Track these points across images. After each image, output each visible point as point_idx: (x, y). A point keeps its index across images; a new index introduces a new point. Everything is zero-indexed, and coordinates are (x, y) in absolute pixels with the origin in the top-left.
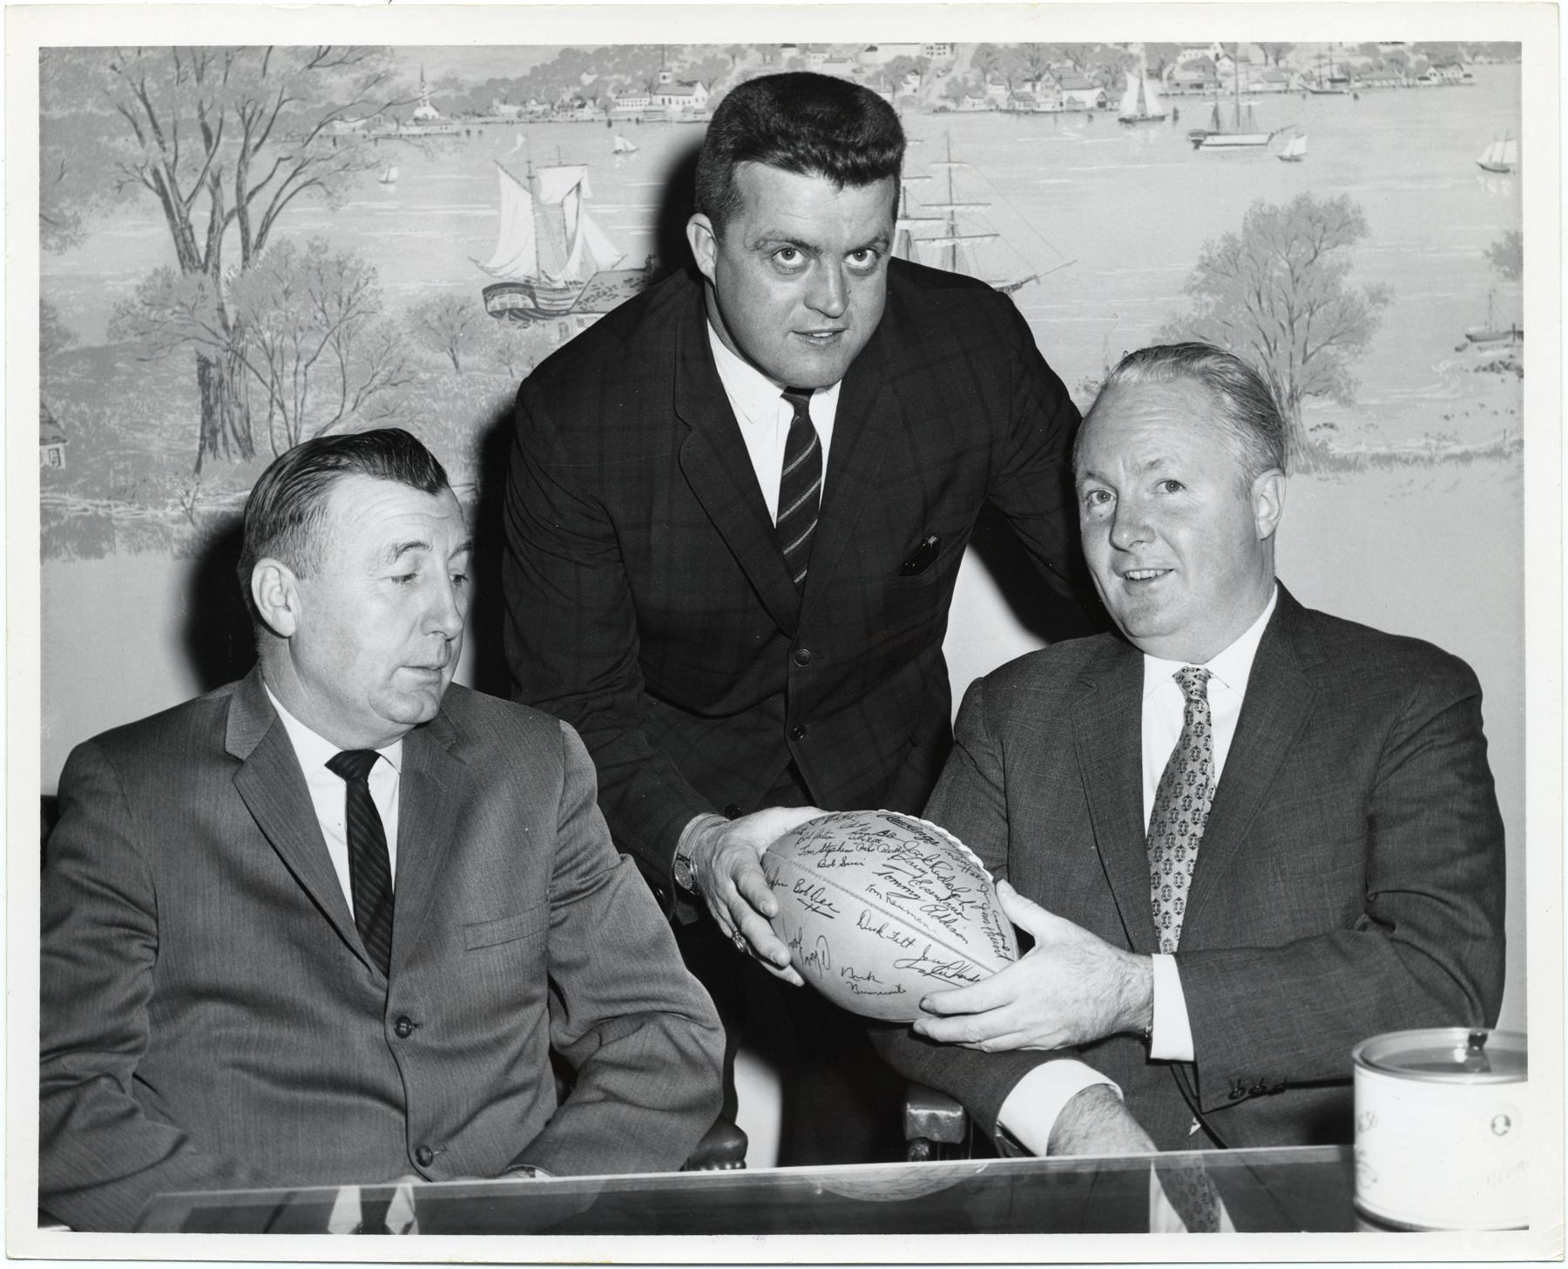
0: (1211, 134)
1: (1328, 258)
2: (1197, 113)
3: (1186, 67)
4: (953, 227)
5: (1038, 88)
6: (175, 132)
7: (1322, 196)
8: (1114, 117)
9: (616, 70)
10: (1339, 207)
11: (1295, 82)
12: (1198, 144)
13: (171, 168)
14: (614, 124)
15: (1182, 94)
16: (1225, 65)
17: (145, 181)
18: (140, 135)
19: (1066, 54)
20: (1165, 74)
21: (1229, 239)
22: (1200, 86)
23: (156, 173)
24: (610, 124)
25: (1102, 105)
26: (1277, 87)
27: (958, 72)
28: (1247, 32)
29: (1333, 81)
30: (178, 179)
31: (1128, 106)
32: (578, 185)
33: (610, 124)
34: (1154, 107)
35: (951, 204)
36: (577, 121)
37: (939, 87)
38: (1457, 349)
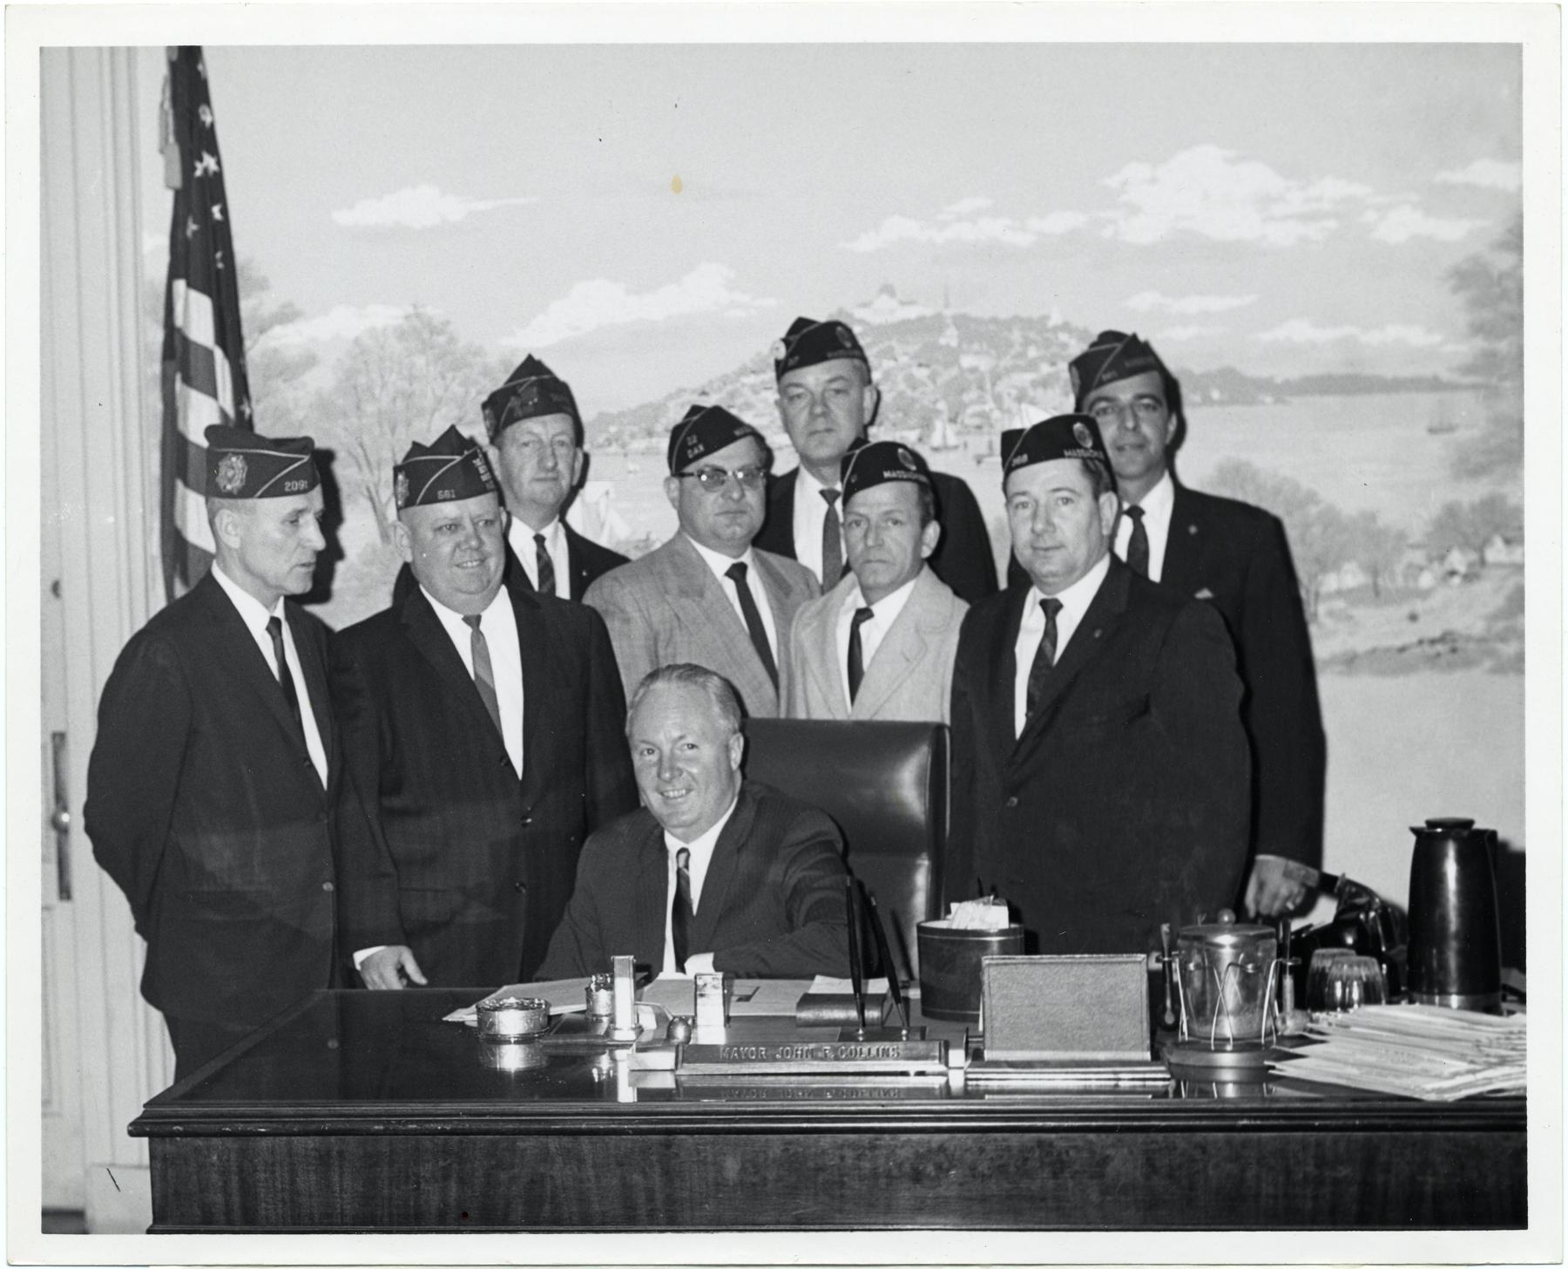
3: (975, 415)
6: (379, 465)
9: (629, 424)
12: (979, 462)
13: (376, 485)
14: (630, 456)
15: (969, 433)
16: (996, 414)
17: (362, 493)
18: (359, 466)
19: (898, 410)
20: (959, 420)
22: (979, 427)
23: (368, 489)
24: (625, 455)
25: (920, 440)
30: (380, 491)
32: (607, 493)
33: (625, 455)
34: (952, 440)
36: (607, 455)
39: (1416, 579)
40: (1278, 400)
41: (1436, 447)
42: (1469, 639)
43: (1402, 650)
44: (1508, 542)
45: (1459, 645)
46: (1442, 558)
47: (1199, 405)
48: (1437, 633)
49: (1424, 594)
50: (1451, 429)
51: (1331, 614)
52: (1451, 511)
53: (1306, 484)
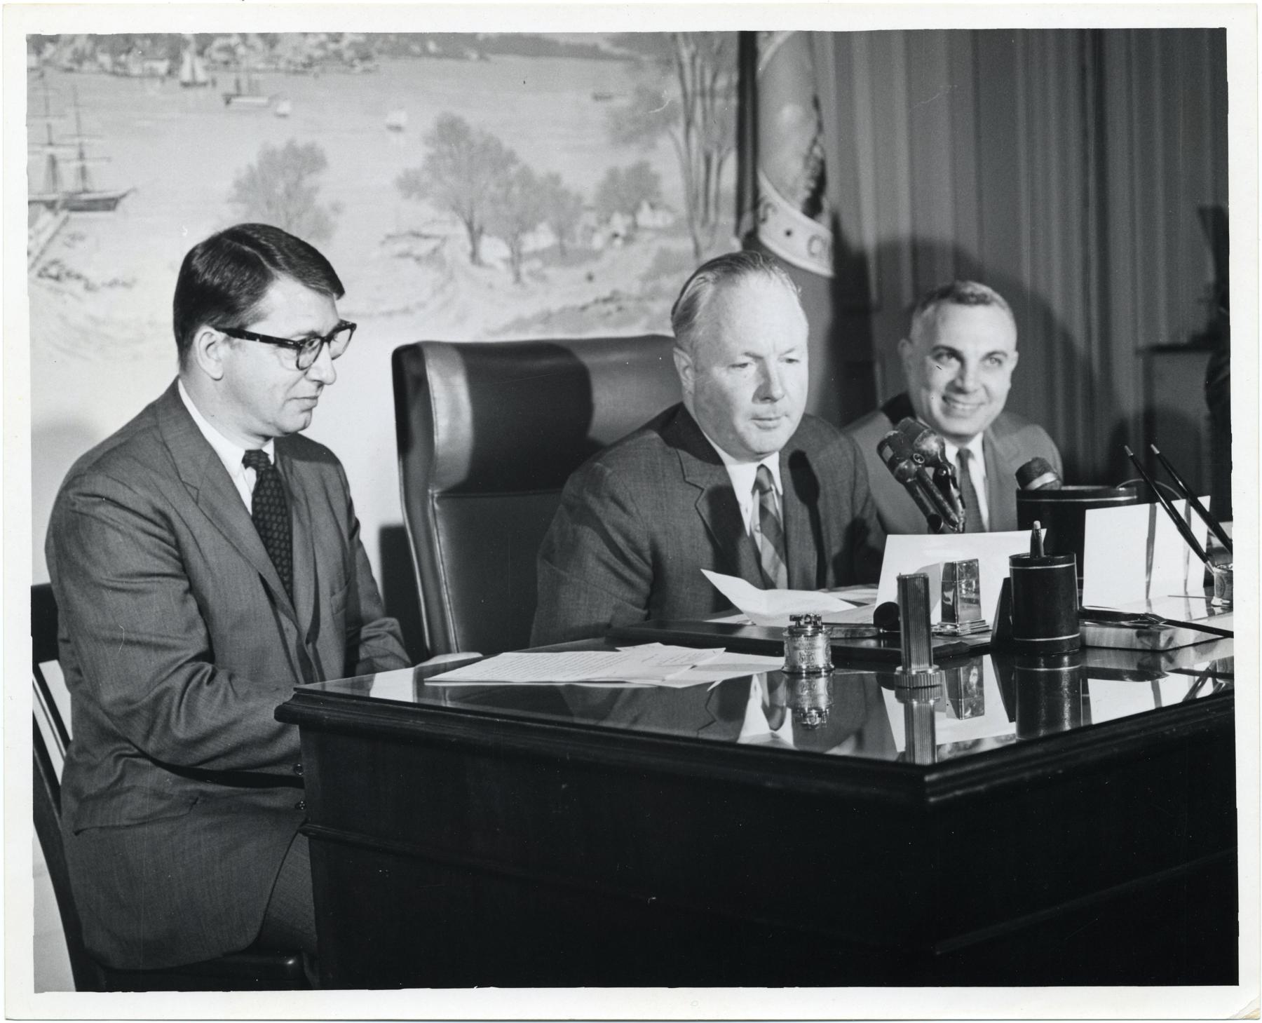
0: (238, 95)
1: (308, 182)
2: (226, 83)
3: (221, 49)
4: (81, 156)
5: (131, 57)
7: (302, 141)
8: (177, 81)
10: (310, 149)
11: (282, 65)
12: (228, 102)
15: (215, 69)
16: (241, 50)
20: (207, 52)
21: (250, 167)
22: (226, 63)
25: (170, 72)
26: (273, 67)
27: (79, 44)
28: (253, 28)
29: (304, 65)
31: (185, 74)
34: (201, 76)
35: (79, 135)
37: (67, 53)
38: (383, 243)
39: (590, 239)
40: (481, 57)
41: (598, 113)
42: (629, 298)
43: (584, 308)
44: (652, 206)
45: (624, 303)
46: (608, 221)
47: (419, 56)
48: (607, 294)
49: (596, 255)
50: (609, 97)
51: (531, 274)
52: (613, 175)
53: (507, 145)
